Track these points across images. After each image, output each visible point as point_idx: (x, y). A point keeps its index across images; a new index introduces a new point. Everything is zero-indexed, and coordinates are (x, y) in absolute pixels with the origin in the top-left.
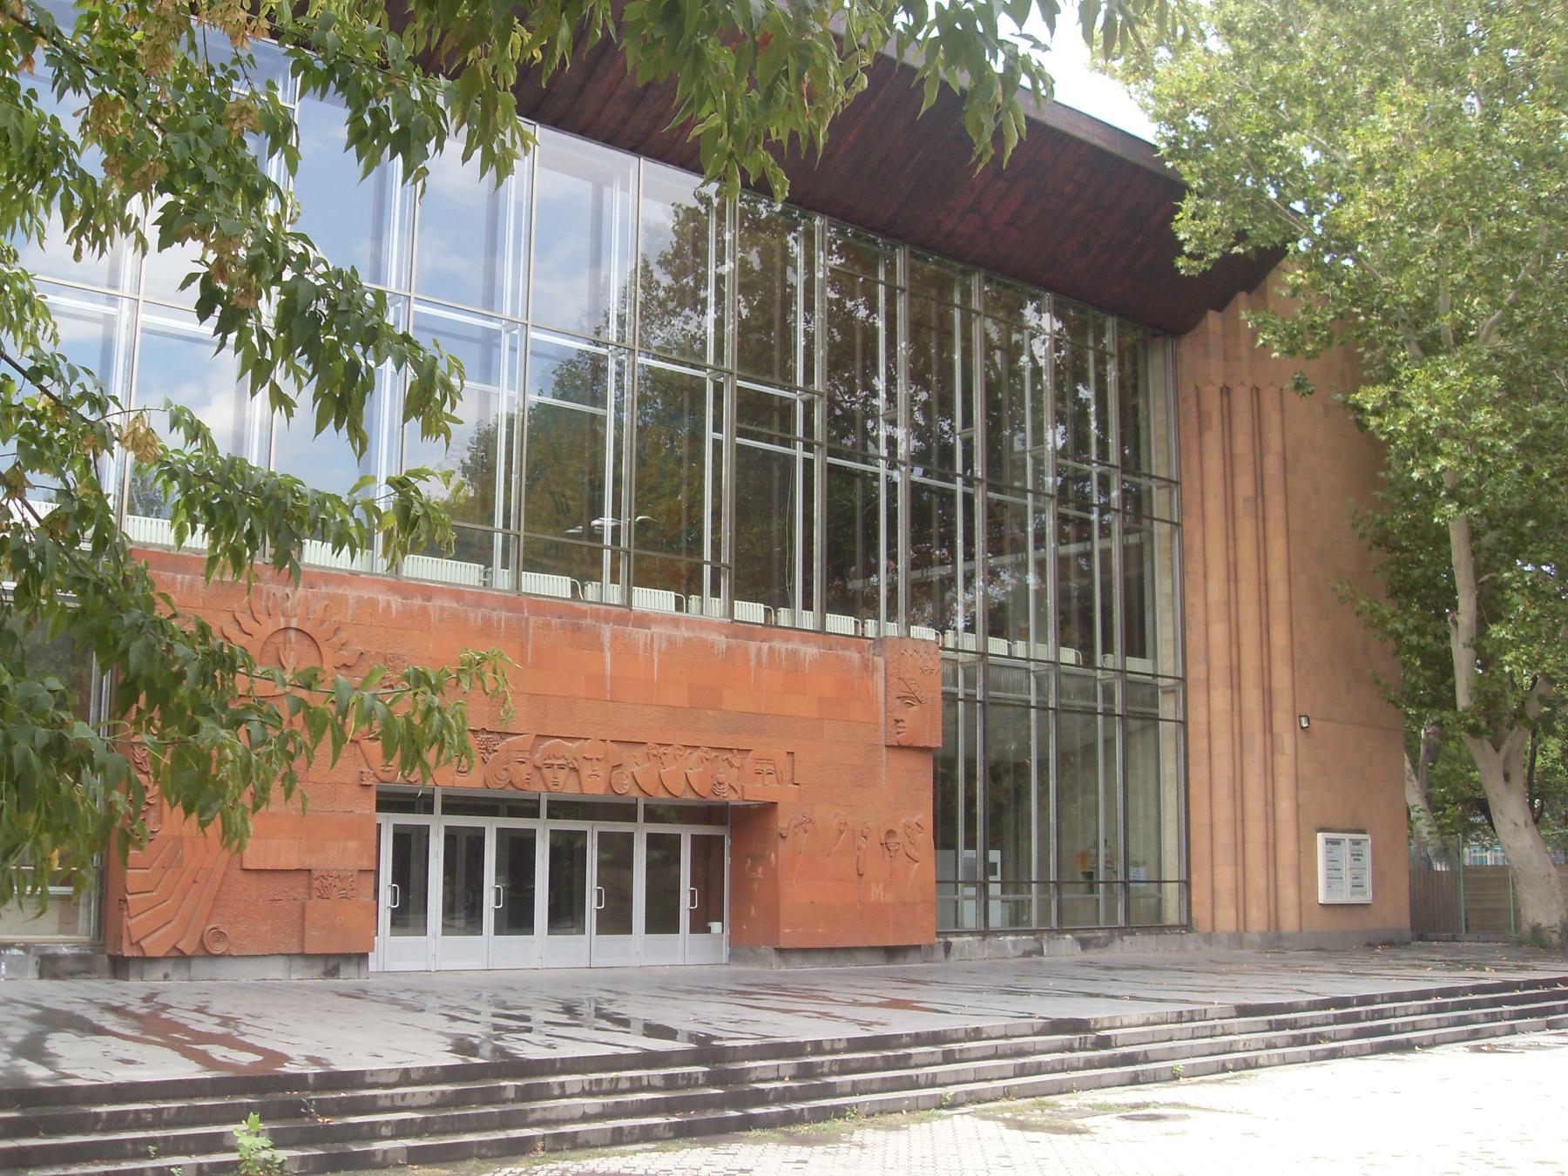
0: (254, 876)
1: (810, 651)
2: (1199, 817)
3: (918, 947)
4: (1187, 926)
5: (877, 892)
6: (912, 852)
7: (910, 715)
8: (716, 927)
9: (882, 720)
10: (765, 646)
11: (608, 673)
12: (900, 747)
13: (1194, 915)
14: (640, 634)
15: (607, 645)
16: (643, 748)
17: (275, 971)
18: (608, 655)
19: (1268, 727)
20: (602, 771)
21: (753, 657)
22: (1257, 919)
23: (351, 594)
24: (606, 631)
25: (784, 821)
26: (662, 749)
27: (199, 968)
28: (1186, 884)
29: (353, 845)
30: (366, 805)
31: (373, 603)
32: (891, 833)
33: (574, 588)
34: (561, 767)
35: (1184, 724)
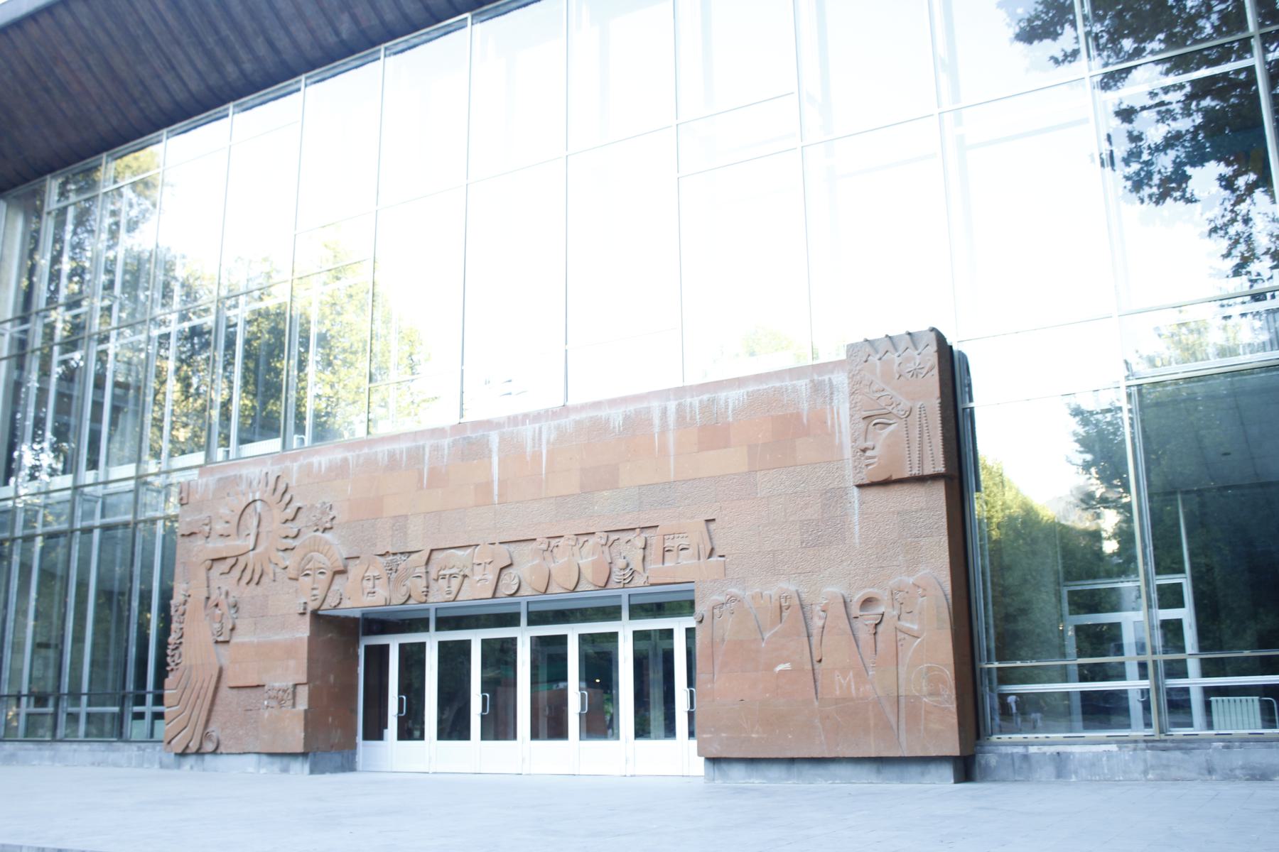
0: (235, 691)
5: (840, 683)
6: (906, 624)
9: (848, 453)
16: (534, 544)
18: (495, 460)
20: (491, 577)
21: (657, 421)
24: (494, 438)
26: (554, 542)
29: (292, 663)
32: (868, 602)
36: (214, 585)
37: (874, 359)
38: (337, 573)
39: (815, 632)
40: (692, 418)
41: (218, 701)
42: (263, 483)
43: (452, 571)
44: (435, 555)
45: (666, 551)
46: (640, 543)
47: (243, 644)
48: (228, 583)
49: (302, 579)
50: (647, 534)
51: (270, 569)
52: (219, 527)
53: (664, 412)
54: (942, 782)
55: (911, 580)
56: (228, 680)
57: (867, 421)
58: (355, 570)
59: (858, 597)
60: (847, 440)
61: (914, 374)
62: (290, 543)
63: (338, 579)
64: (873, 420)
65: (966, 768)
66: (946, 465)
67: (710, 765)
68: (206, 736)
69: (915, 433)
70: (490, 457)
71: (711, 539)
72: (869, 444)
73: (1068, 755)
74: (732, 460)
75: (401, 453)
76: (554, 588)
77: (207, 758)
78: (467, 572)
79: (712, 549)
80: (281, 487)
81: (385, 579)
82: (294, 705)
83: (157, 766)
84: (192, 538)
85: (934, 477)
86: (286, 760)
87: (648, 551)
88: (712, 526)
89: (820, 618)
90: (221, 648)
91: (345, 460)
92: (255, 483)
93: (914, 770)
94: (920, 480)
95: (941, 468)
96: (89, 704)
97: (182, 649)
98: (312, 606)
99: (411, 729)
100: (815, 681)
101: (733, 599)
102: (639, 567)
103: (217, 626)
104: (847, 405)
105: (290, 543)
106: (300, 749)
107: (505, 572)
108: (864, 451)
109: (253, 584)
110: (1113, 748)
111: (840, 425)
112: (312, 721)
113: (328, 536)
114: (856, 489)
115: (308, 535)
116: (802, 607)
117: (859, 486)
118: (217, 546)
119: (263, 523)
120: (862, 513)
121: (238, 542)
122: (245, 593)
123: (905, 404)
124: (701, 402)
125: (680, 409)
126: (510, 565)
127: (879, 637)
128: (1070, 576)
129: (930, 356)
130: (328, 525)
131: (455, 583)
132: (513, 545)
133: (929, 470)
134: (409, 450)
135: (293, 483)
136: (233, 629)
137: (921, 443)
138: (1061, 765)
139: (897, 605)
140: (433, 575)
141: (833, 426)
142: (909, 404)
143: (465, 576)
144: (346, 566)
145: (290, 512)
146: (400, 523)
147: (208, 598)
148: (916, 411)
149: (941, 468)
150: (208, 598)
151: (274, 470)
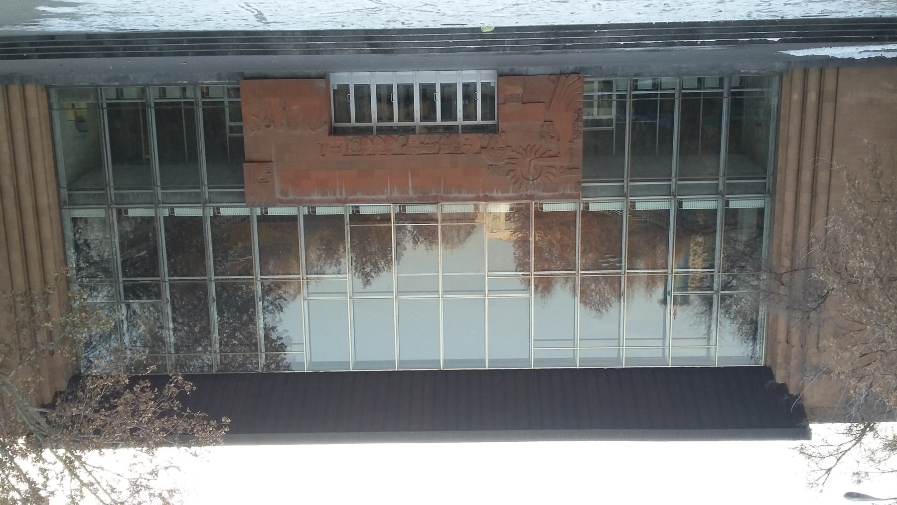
1: (316, 197)
2: (47, 142)
3: (246, 78)
4: (47, 88)
8: (336, 88)
9: (275, 173)
10: (338, 196)
13: (45, 94)
14: (396, 194)
17: (532, 70)
18: (410, 184)
19: (17, 188)
21: (344, 191)
22: (15, 90)
23: (511, 194)
24: (411, 193)
25: (326, 127)
27: (558, 72)
28: (50, 107)
30: (502, 126)
31: (503, 192)
32: (268, 126)
33: (405, 210)
35: (59, 186)
46: (350, 150)
49: (504, 146)
53: (341, 194)
58: (477, 148)
70: (413, 186)
94: (252, 162)
113: (491, 163)
118: (556, 162)
134: (451, 193)
138: (219, 77)
149: (246, 166)
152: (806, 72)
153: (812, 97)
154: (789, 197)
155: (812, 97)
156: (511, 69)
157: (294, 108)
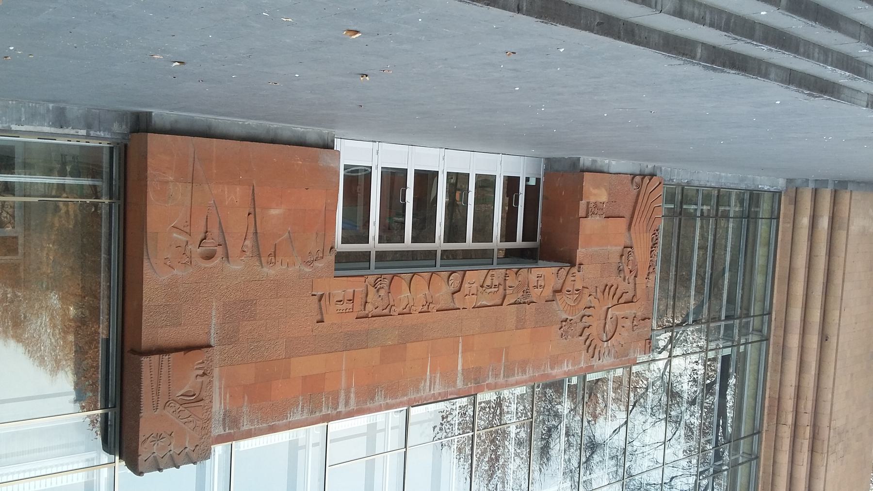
0: (621, 215)
6: (183, 238)
7: (190, 383)
9: (216, 372)
11: (460, 356)
12: (188, 348)
15: (460, 375)
16: (438, 307)
18: (460, 368)
20: (466, 285)
21: (352, 395)
24: (460, 384)
26: (425, 308)
32: (209, 257)
34: (489, 287)
36: (632, 285)
37: (190, 448)
38: (560, 291)
39: (250, 235)
40: (327, 399)
41: (631, 209)
42: (602, 353)
43: (489, 290)
44: (499, 302)
45: (352, 300)
46: (369, 307)
47: (616, 246)
48: (623, 286)
50: (363, 313)
51: (599, 295)
52: (628, 323)
53: (347, 403)
54: (161, 114)
55: (175, 272)
56: (623, 223)
57: (200, 397)
58: (548, 292)
59: (216, 261)
60: (216, 383)
61: (160, 437)
62: (588, 312)
63: (559, 287)
64: (195, 399)
65: (141, 125)
66: (140, 362)
67: (330, 144)
68: (639, 186)
69: (163, 388)
70: (463, 370)
71: (321, 308)
72: (200, 380)
73: (54, 125)
74: (304, 366)
75: (518, 373)
76: (427, 276)
77: (638, 172)
78: (481, 289)
79: (320, 300)
80: (591, 350)
81: (531, 286)
82: (588, 203)
83: (663, 168)
84: (644, 316)
85: (149, 352)
86: (593, 168)
87: (364, 300)
88: (319, 318)
89: (247, 246)
90: (628, 243)
91: (552, 368)
92: (606, 353)
93: (182, 125)
94: (162, 351)
95: (145, 360)
96: (729, 211)
97: (651, 244)
98: (575, 270)
99: (512, 183)
100: (254, 199)
101: (309, 263)
102: (371, 289)
103: (631, 258)
104: (213, 410)
105: (588, 312)
106: (586, 174)
107: (457, 289)
108: (204, 374)
109: (609, 285)
110: (14, 127)
111: (220, 394)
112: (578, 192)
113: (564, 316)
114: (212, 343)
115: (576, 318)
116: (259, 256)
117: (209, 346)
118: (629, 310)
119: (602, 325)
120: (209, 325)
121: (617, 313)
122: (613, 280)
123: (168, 412)
124: (321, 411)
125: (336, 406)
126: (453, 294)
127: (203, 229)
128: (15, 267)
129: (144, 452)
130: (564, 323)
131: (488, 282)
132: (451, 307)
133: (155, 358)
134: (513, 375)
135: (584, 353)
136: (622, 255)
137: (159, 380)
138: (61, 119)
139: (188, 253)
140: (501, 287)
141: (225, 394)
142: (165, 411)
143: (482, 286)
144: (554, 296)
145: (587, 332)
146: (520, 324)
147: (635, 277)
148: (160, 406)
150: (635, 277)
151: (595, 362)
152: (816, 193)
153: (824, 223)
154: (794, 341)
155: (824, 223)
156: (594, 161)
157: (274, 212)
